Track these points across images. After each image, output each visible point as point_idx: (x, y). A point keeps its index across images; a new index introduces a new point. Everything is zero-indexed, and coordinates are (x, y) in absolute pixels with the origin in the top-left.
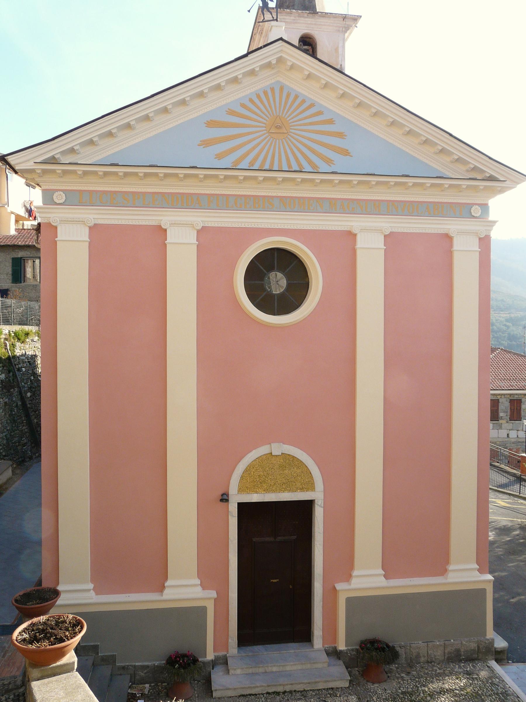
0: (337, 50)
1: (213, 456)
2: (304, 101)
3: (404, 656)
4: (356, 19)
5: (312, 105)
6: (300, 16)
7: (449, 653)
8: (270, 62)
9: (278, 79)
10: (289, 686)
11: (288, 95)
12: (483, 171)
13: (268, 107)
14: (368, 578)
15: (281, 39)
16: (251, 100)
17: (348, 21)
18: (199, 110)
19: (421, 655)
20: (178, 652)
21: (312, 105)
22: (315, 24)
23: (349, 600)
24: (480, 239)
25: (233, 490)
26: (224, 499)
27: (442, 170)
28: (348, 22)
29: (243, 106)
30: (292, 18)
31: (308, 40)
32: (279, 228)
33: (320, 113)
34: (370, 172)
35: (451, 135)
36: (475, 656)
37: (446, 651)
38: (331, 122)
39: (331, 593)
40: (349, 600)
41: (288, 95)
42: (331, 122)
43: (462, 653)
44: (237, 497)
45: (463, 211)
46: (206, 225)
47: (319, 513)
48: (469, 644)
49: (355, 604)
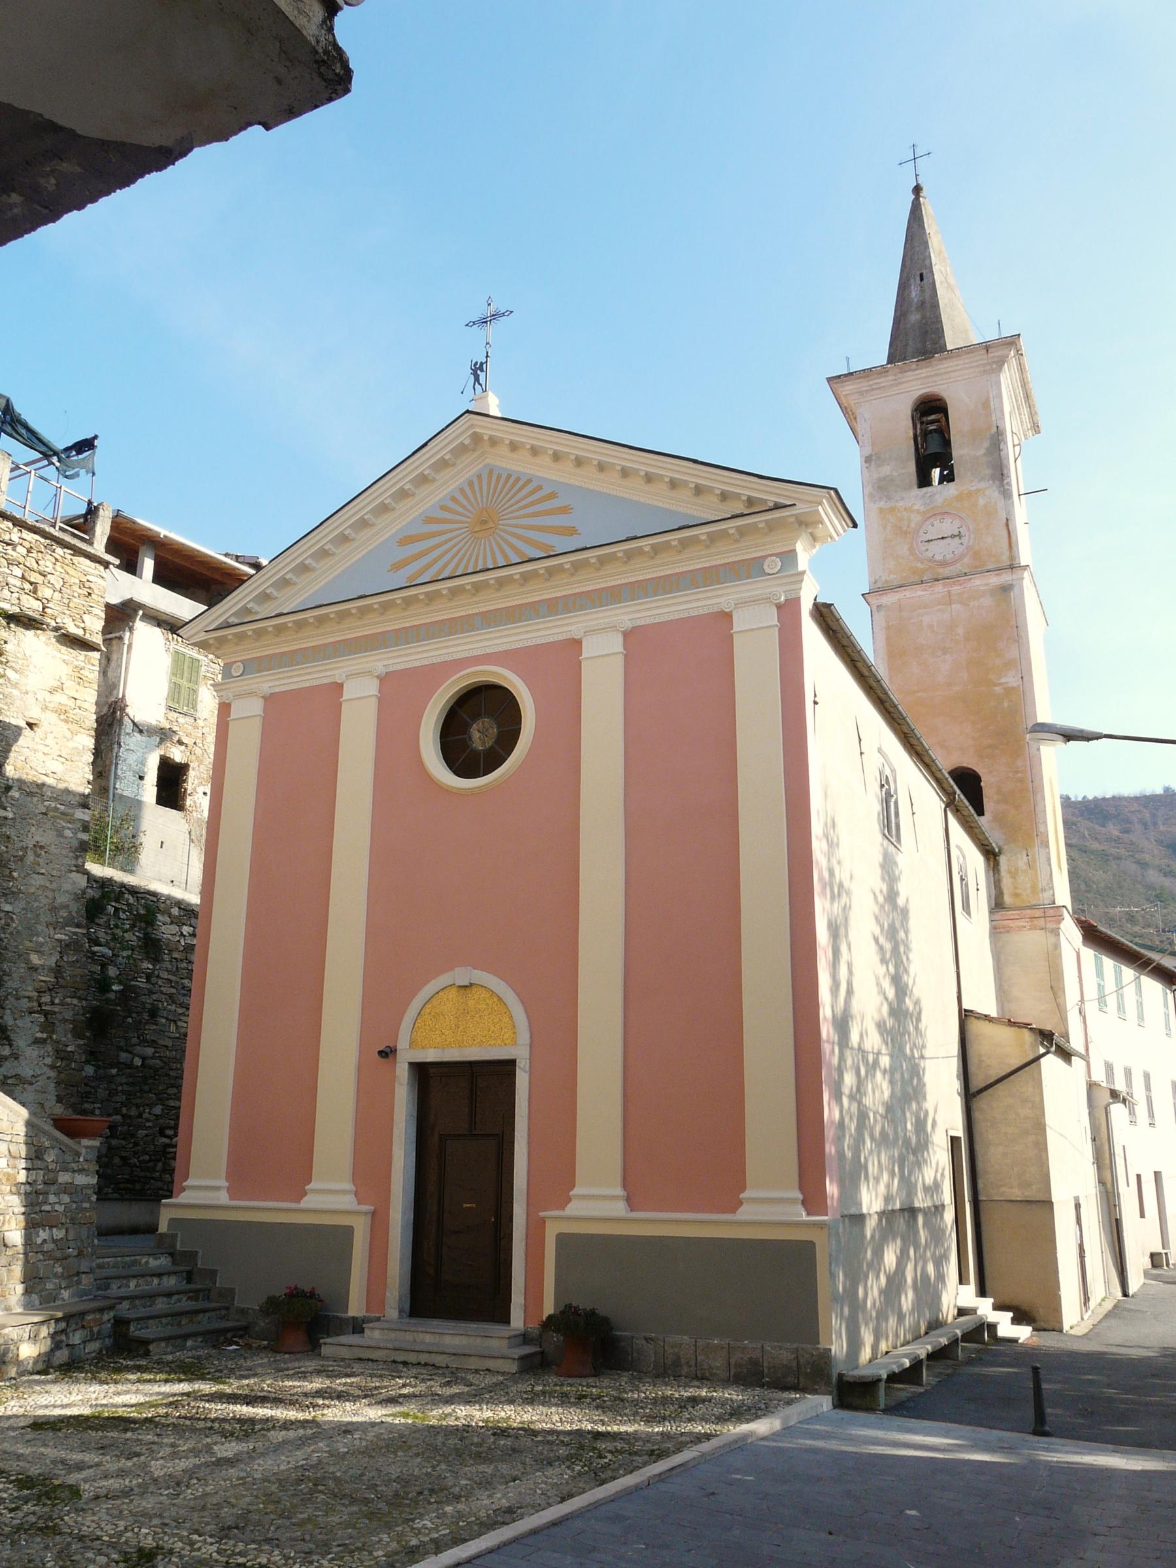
0: (986, 404)
1: (385, 992)
2: (518, 479)
3: (652, 1359)
4: (1012, 342)
5: (529, 481)
6: (903, 371)
7: (738, 1365)
8: (462, 444)
9: (487, 461)
10: (427, 1355)
11: (499, 477)
12: (765, 501)
13: (520, 504)
14: (597, 1201)
15: (468, 411)
16: (454, 499)
17: (1000, 350)
18: (389, 528)
19: (683, 1361)
20: (296, 1288)
21: (529, 481)
22: (937, 375)
23: (562, 1239)
24: (779, 607)
25: (402, 1044)
26: (388, 1053)
27: (695, 513)
28: (995, 354)
29: (443, 508)
30: (890, 378)
31: (934, 404)
32: (478, 653)
33: (540, 488)
34: (580, 547)
35: (695, 461)
36: (791, 1380)
37: (732, 1361)
38: (552, 496)
39: (536, 1228)
40: (562, 1239)
41: (499, 477)
42: (552, 496)
43: (766, 1371)
44: (407, 1055)
45: (752, 569)
46: (391, 669)
47: (522, 1080)
48: (780, 1353)
49: (576, 1250)
